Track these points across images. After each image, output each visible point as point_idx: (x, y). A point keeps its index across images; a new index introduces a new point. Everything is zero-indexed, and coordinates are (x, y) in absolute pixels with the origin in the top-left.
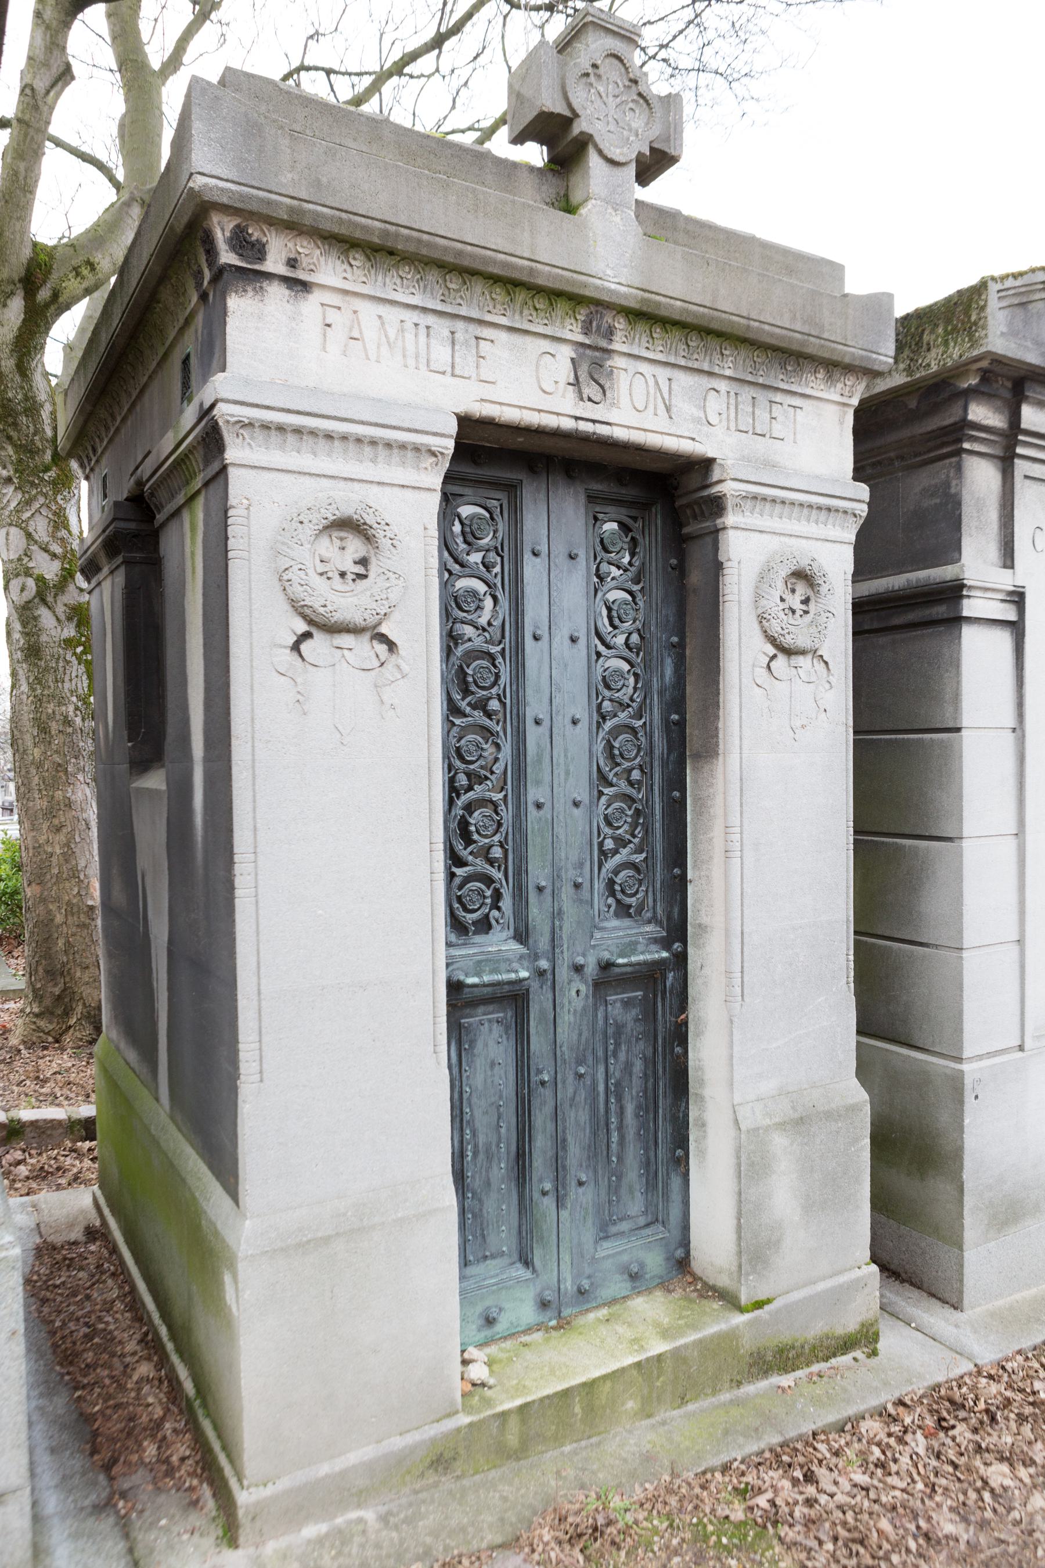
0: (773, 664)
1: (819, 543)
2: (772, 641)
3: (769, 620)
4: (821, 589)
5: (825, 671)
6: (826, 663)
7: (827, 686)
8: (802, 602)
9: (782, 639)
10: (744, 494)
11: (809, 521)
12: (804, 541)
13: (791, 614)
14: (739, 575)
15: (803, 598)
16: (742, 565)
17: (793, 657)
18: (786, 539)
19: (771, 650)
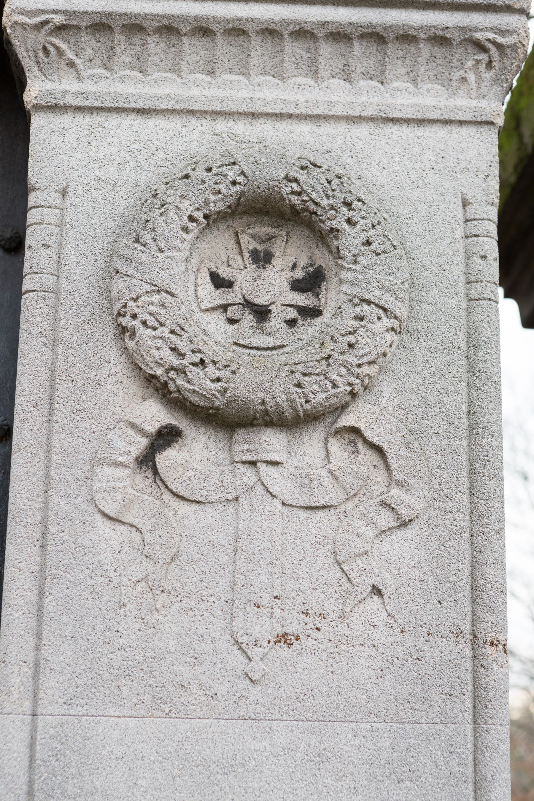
0: (167, 459)
1: (363, 130)
2: (159, 388)
3: (133, 336)
4: (342, 242)
5: (380, 475)
6: (379, 450)
7: (386, 519)
8: (297, 286)
9: (180, 381)
10: (58, 19)
11: (315, 74)
12: (304, 129)
13: (249, 318)
14: (61, 225)
15: (299, 274)
16: (71, 198)
17: (240, 435)
18: (240, 127)
19: (155, 415)
